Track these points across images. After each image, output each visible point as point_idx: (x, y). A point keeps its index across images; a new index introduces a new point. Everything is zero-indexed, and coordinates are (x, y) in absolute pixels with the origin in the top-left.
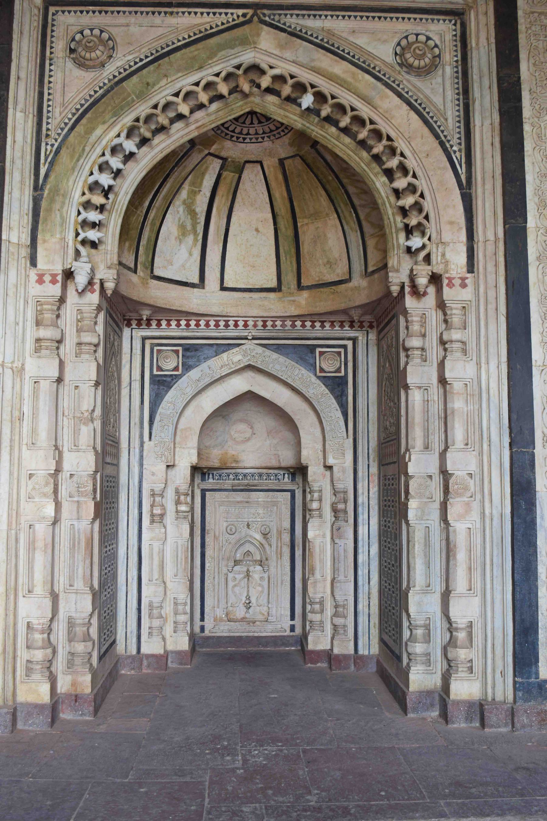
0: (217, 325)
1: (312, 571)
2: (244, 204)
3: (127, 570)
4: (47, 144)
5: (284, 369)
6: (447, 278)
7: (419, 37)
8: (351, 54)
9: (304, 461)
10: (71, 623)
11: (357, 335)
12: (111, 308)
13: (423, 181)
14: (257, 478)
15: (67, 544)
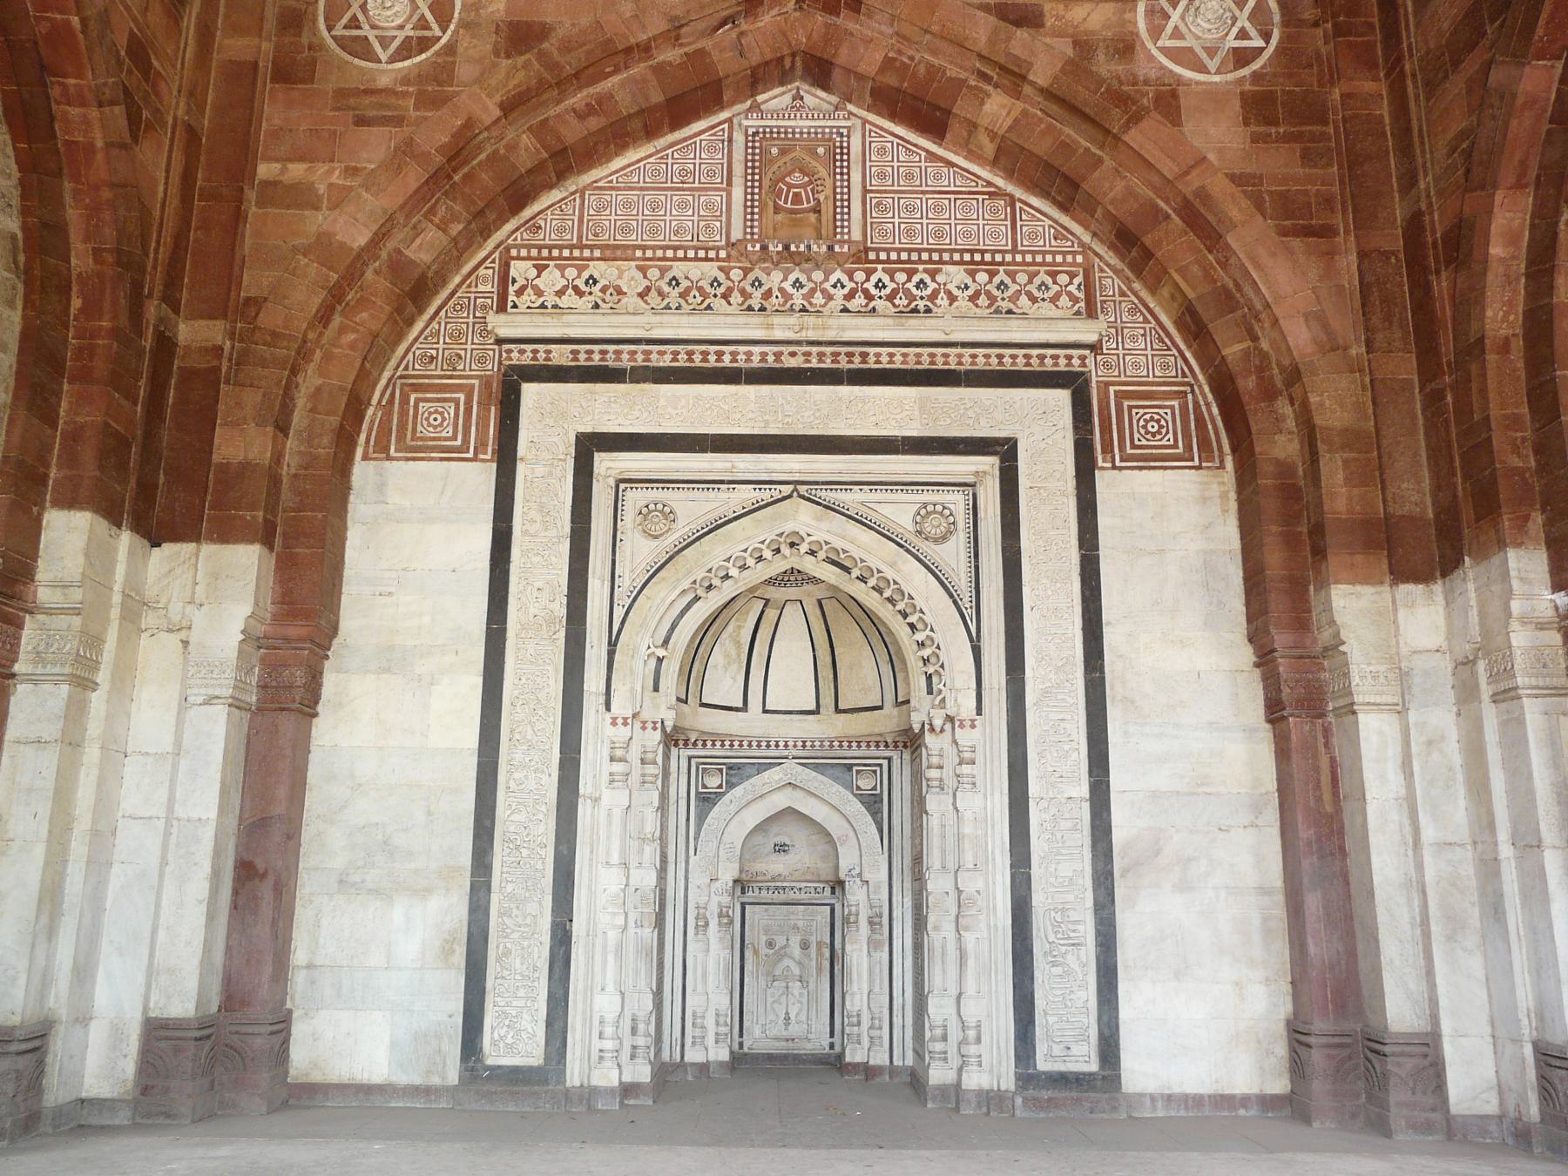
9: (842, 876)
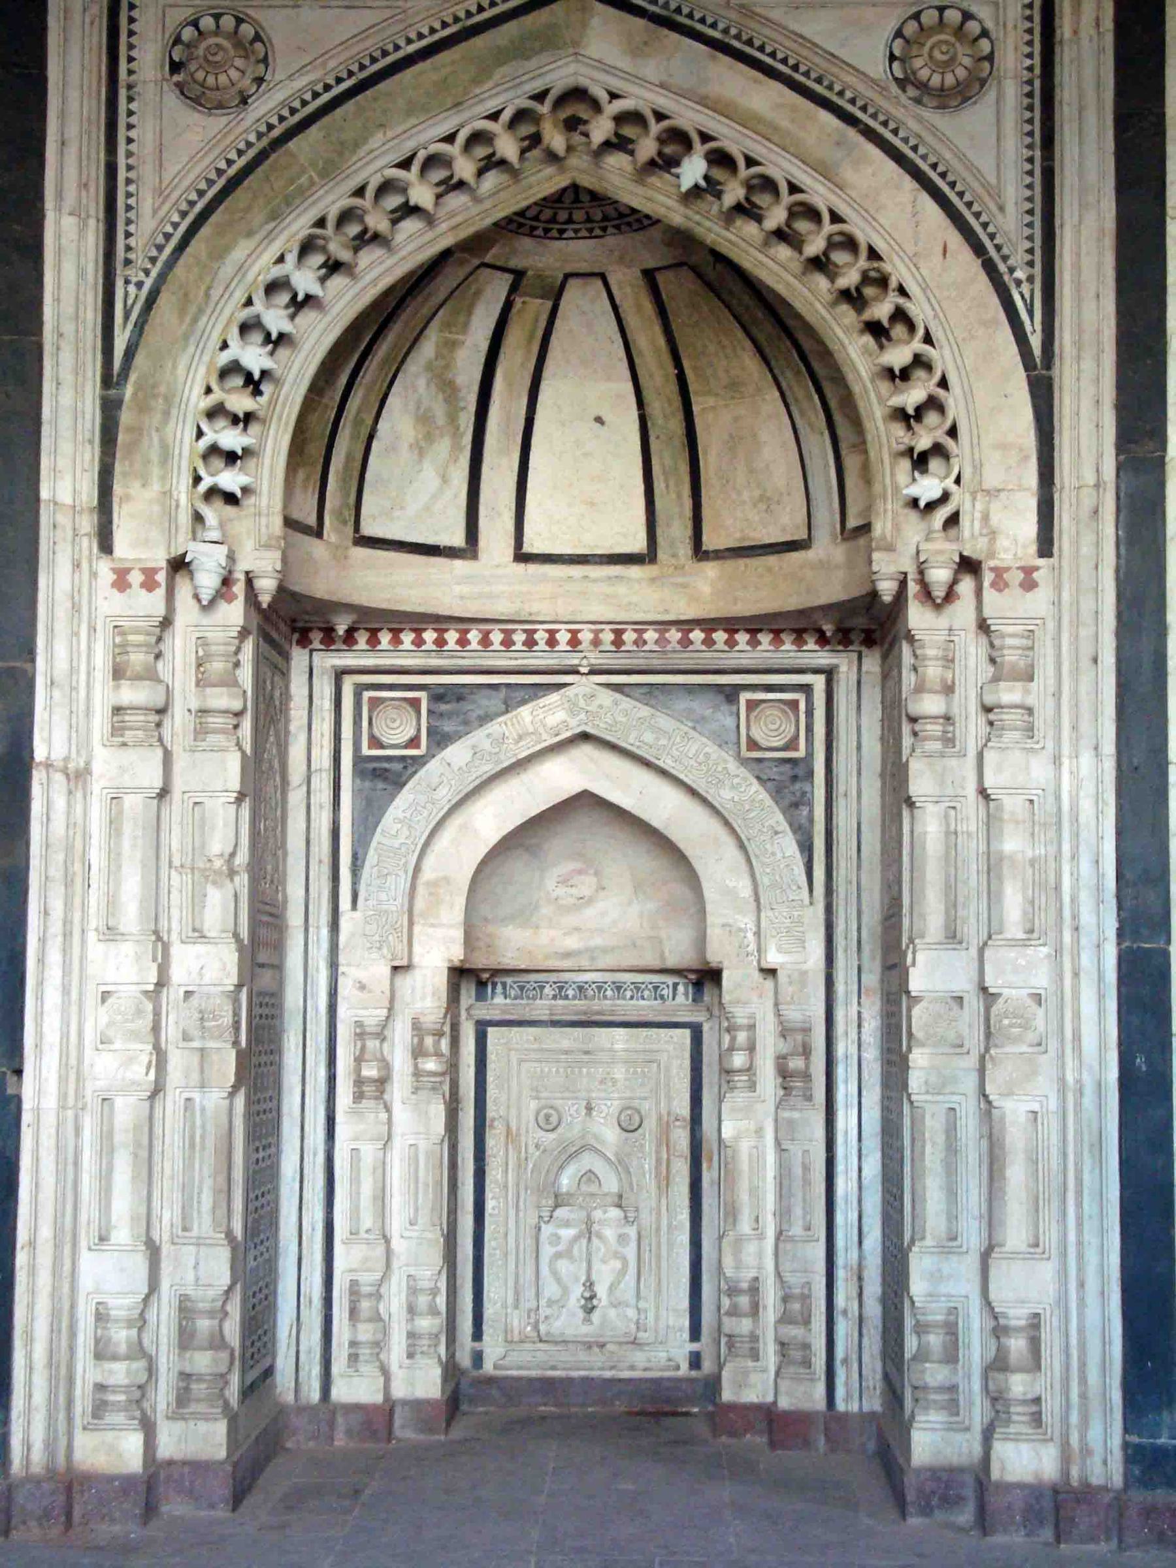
0: (508, 643)
2: (568, 362)
3: (300, 1208)
4: (127, 282)
6: (992, 569)
8: (791, 62)
9: (714, 957)
10: (186, 1309)
11: (835, 661)
13: (947, 352)
14: (609, 993)
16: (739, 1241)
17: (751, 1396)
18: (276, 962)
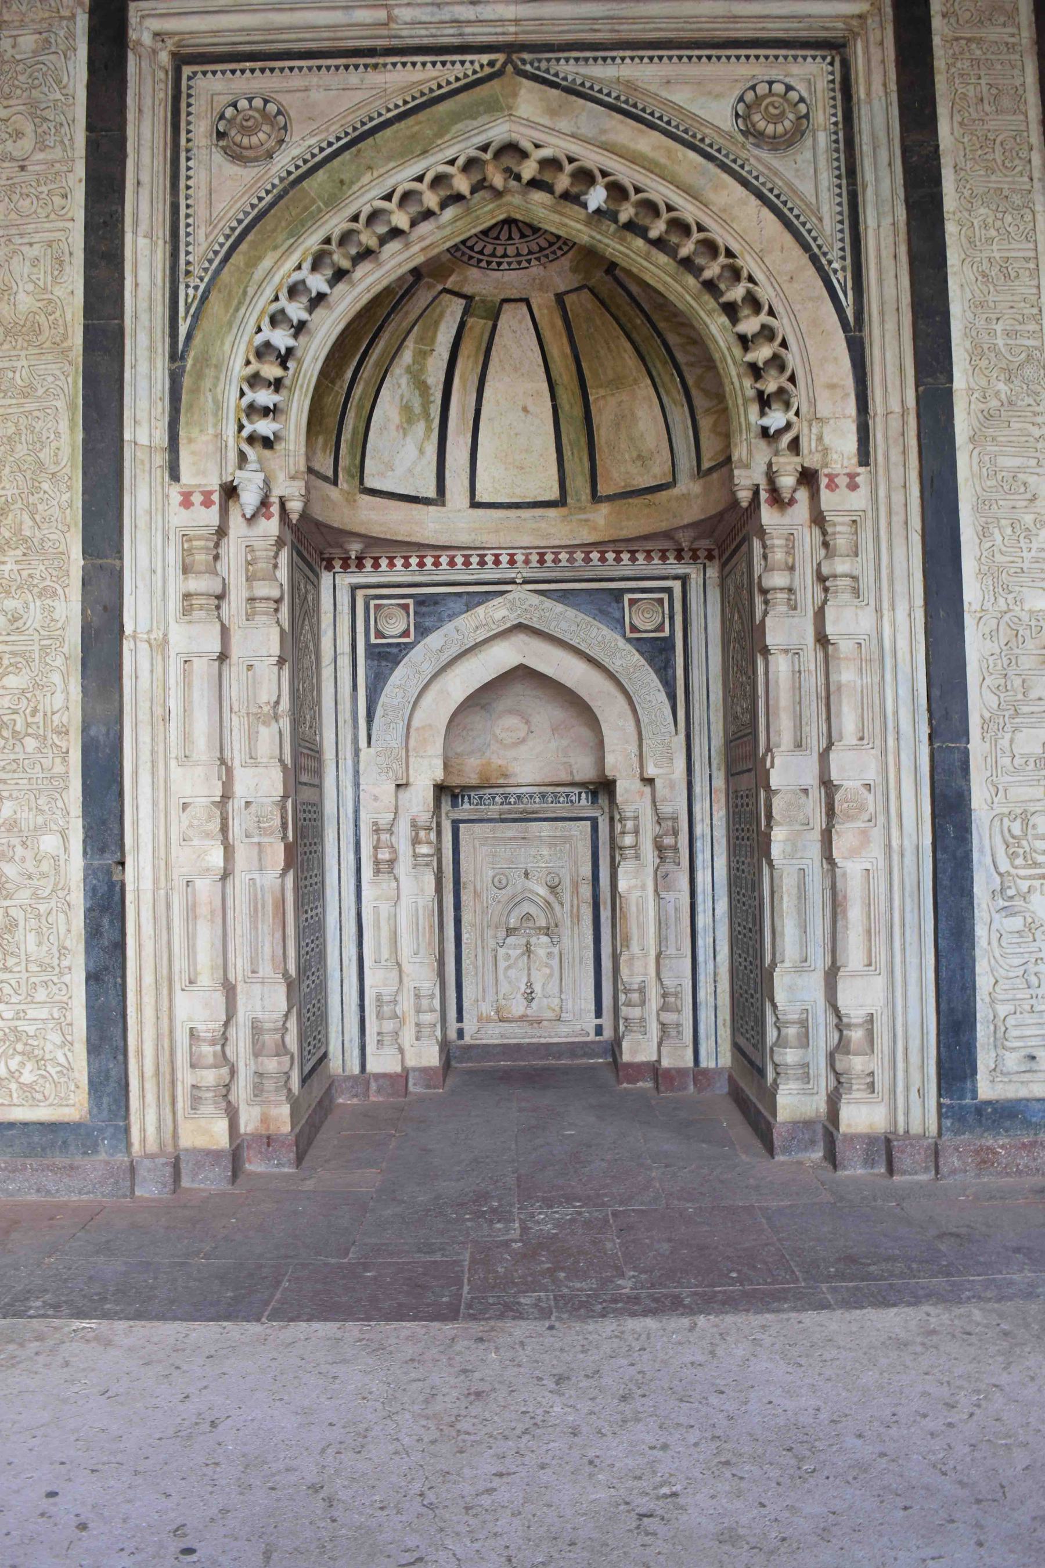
0: (467, 563)
1: (627, 941)
2: (503, 369)
4: (187, 286)
5: (574, 628)
7: (774, 86)
8: (665, 119)
10: (256, 1029)
11: (687, 571)
12: (299, 541)
13: (785, 321)
15: (245, 910)
16: (632, 958)
17: (642, 1058)
18: (316, 782)
